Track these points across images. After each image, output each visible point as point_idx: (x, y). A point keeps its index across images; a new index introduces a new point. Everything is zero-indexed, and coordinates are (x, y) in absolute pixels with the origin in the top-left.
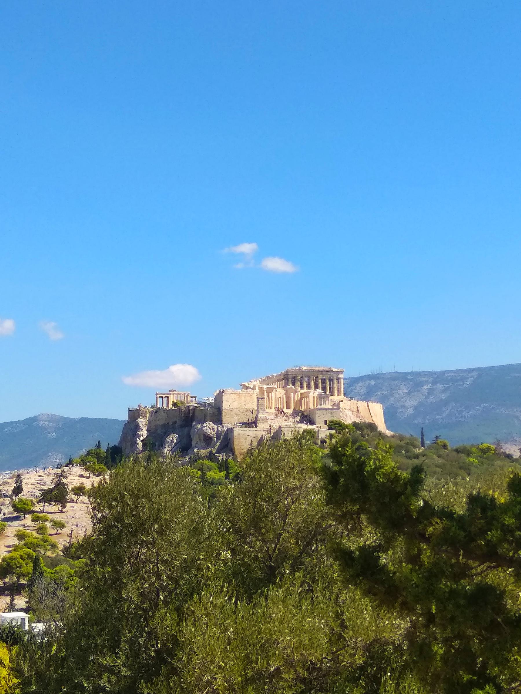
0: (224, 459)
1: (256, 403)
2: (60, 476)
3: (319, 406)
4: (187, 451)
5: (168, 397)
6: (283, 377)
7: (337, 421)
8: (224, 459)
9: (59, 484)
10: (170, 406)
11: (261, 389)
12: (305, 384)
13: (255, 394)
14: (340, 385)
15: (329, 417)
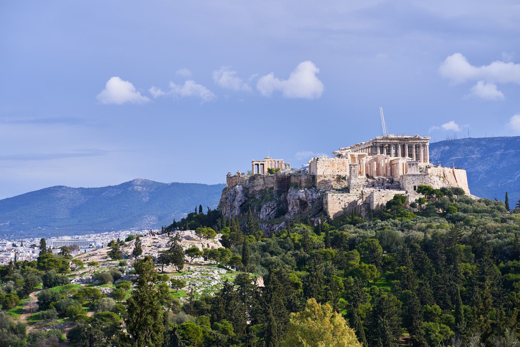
1: (348, 170)
3: (408, 173)
4: (284, 215)
5: (263, 164)
6: (371, 145)
7: (426, 187)
9: (174, 247)
11: (353, 157)
12: (393, 151)
13: (348, 161)
14: (427, 153)
15: (417, 184)
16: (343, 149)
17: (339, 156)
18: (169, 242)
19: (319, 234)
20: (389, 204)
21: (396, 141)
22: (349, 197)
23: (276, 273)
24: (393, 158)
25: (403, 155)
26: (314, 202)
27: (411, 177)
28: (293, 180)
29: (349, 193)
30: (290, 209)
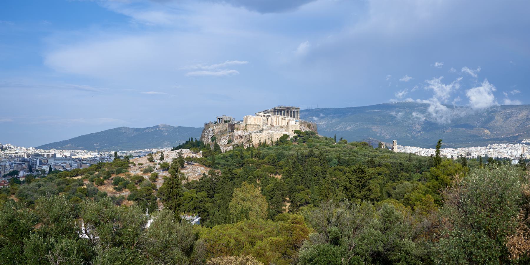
15: (294, 129)
28: (236, 126)
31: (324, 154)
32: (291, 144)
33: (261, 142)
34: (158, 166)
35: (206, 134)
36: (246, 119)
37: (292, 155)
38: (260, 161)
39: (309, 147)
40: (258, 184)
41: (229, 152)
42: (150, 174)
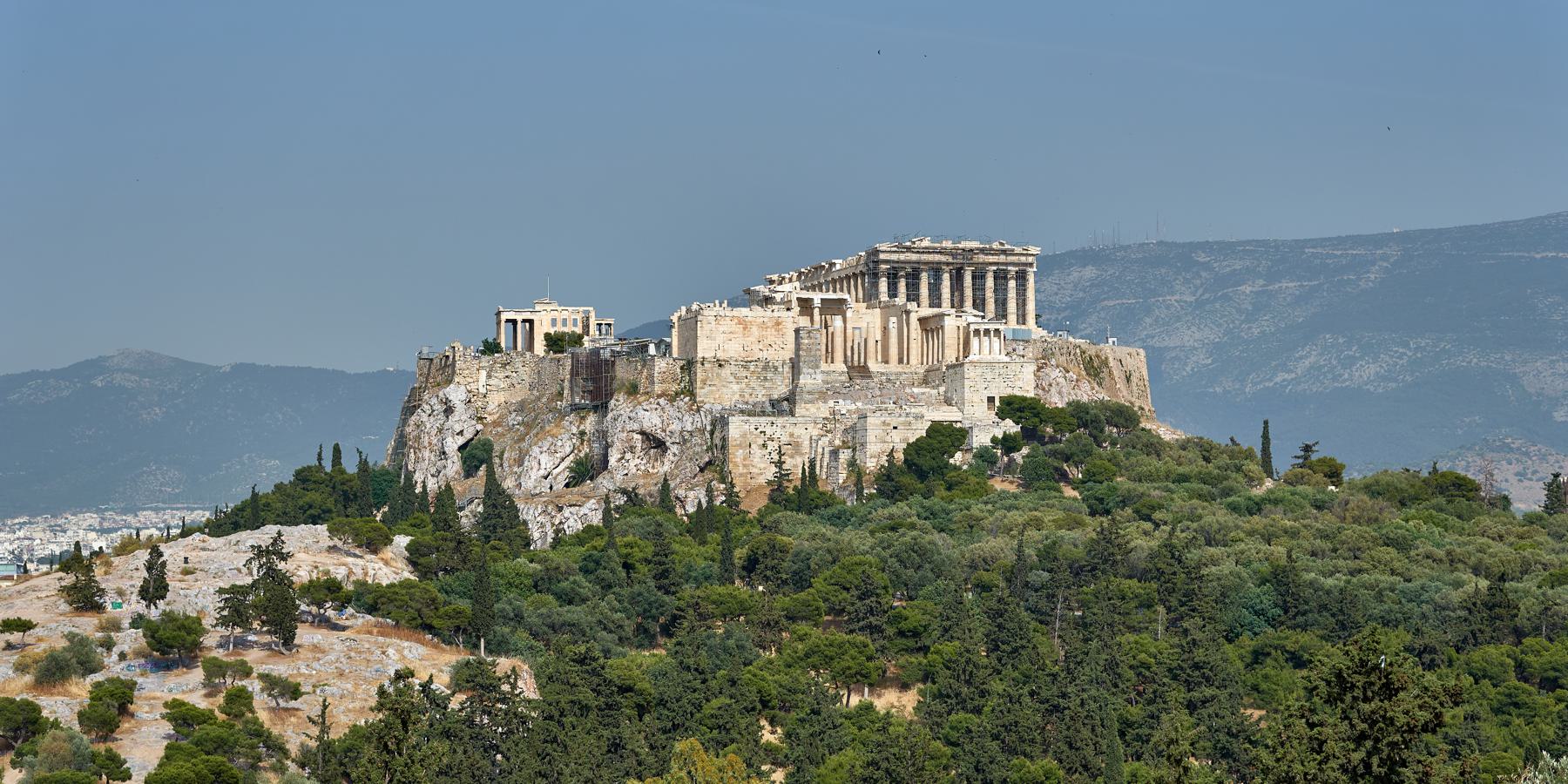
0: (704, 501)
1: (791, 346)
2: (268, 552)
5: (531, 322)
7: (1024, 399)
8: (704, 501)
10: (540, 347)
11: (806, 305)
15: (1000, 390)
16: (775, 277)
17: (767, 301)
18: (249, 561)
19: (703, 543)
20: (914, 449)
21: (937, 258)
22: (790, 429)
23: (582, 660)
24: (926, 311)
25: (958, 304)
26: (685, 441)
27: (979, 371)
28: (622, 372)
29: (792, 414)
30: (613, 461)
31: (1193, 555)
32: (982, 491)
33: (782, 476)
34: (131, 640)
35: (431, 424)
36: (690, 325)
37: (988, 562)
38: (783, 601)
39: (1098, 508)
40: (769, 750)
41: (579, 539)
42: (80, 689)
